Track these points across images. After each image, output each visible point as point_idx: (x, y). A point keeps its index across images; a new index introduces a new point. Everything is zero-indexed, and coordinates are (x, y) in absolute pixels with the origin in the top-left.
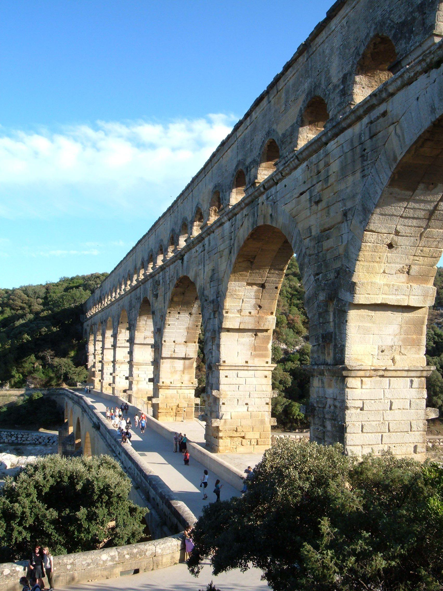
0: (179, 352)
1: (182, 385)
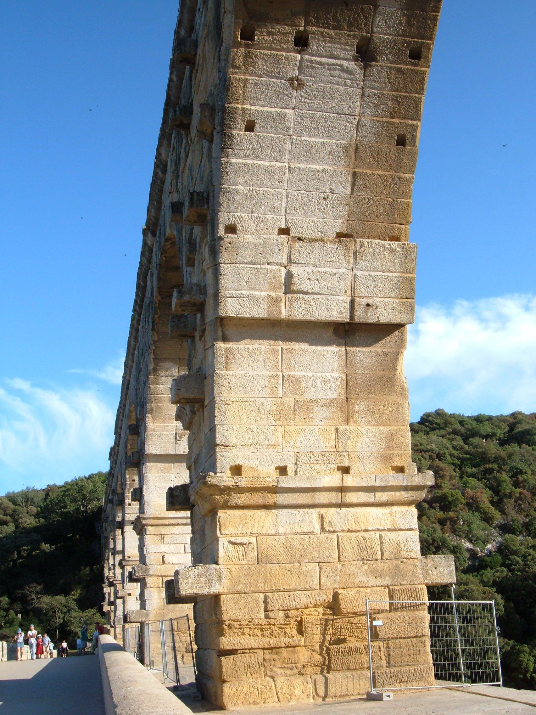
0: (314, 287)
1: (350, 481)
